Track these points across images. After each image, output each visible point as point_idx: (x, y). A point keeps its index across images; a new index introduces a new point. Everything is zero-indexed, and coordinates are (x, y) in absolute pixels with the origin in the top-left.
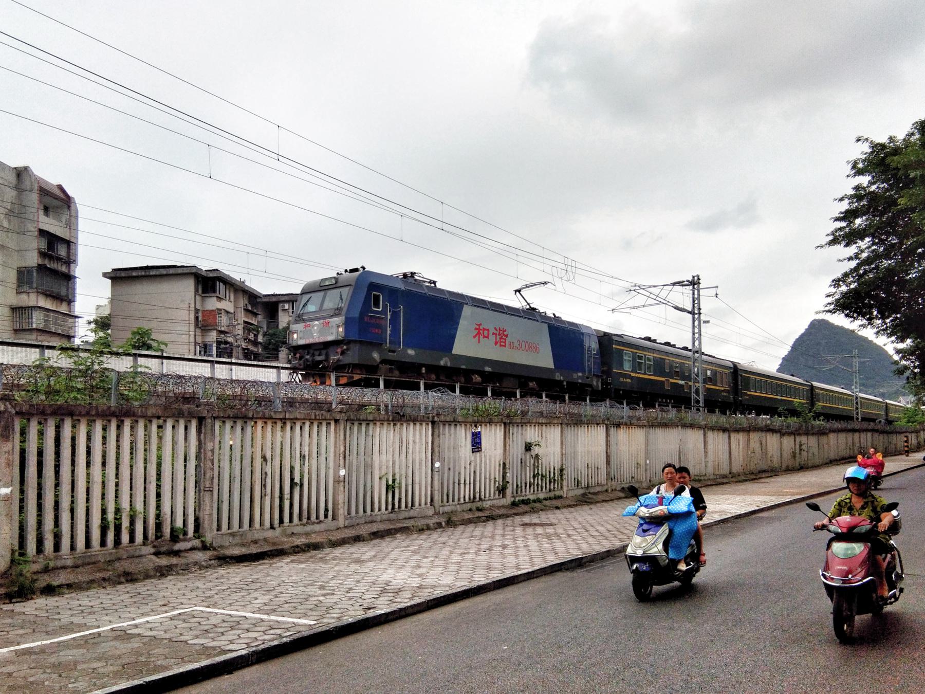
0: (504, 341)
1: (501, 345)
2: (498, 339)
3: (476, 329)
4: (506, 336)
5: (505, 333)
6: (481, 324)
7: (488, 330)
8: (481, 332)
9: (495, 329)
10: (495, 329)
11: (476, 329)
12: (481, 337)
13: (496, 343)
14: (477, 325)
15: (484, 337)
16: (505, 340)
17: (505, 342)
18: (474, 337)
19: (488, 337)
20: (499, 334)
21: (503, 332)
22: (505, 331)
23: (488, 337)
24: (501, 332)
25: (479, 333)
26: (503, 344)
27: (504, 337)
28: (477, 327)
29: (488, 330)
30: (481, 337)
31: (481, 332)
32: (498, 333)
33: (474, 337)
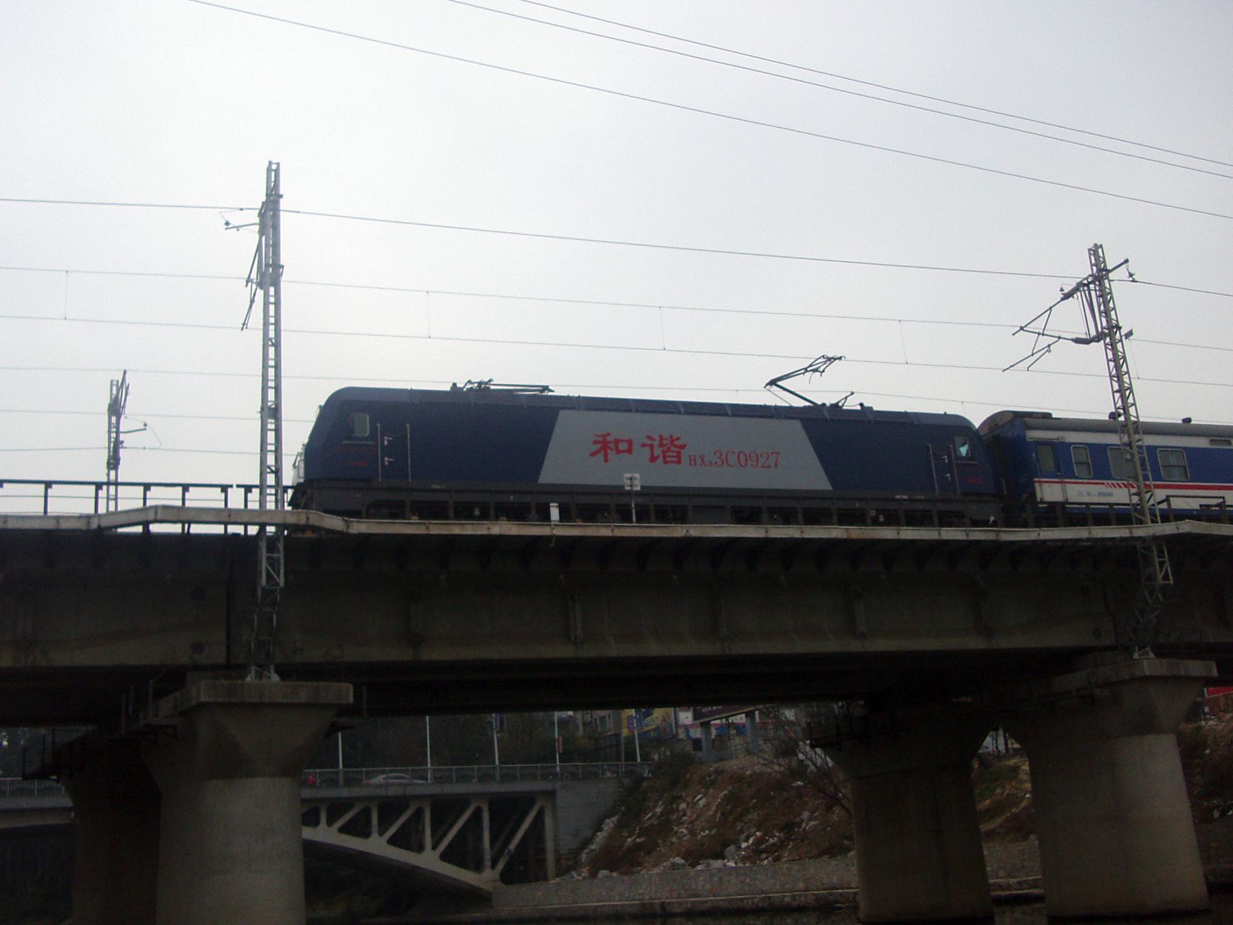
0: (675, 454)
3: (595, 442)
6: (609, 434)
9: (649, 437)
13: (653, 459)
16: (679, 453)
22: (678, 439)
26: (676, 459)
27: (673, 449)
28: (600, 439)
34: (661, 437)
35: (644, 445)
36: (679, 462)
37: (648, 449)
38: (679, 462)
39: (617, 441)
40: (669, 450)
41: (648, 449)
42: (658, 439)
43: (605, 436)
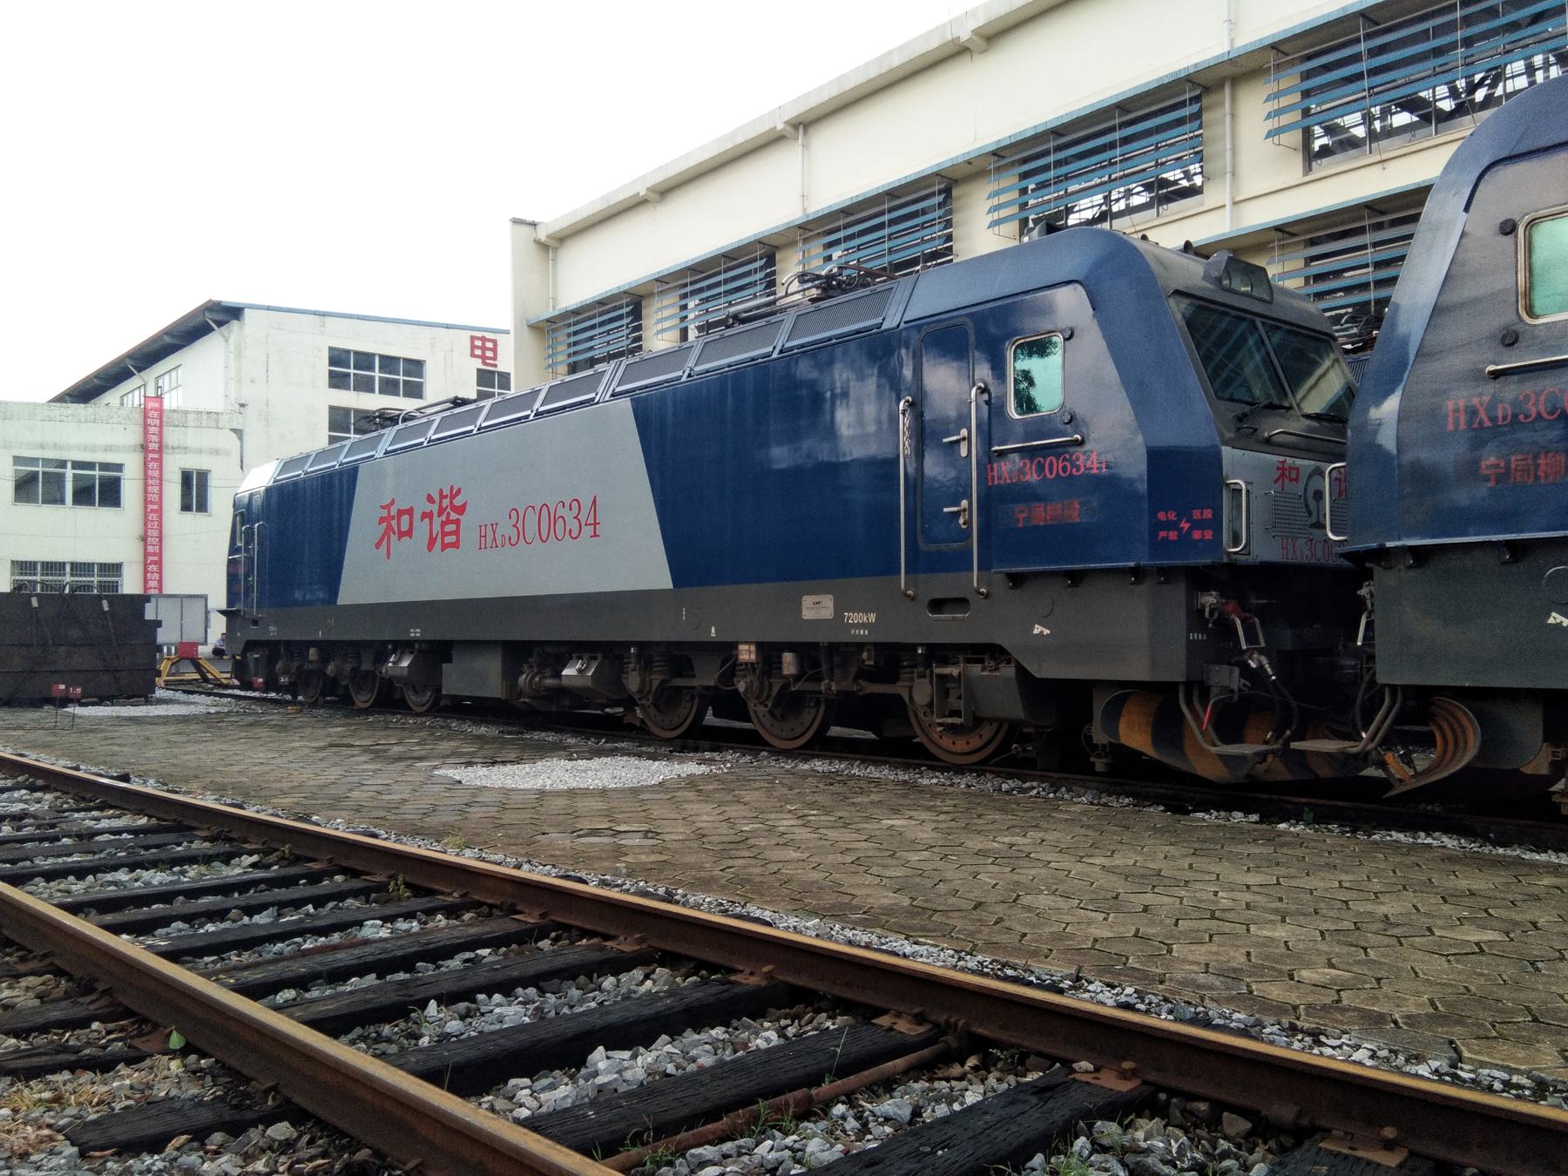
1: (444, 546)
2: (437, 528)
4: (461, 510)
5: (458, 502)
6: (393, 502)
7: (410, 512)
8: (394, 523)
9: (430, 499)
10: (430, 499)
11: (381, 520)
12: (394, 538)
14: (383, 507)
15: (401, 535)
16: (457, 522)
17: (456, 533)
18: (378, 545)
19: (409, 533)
20: (440, 514)
21: (453, 497)
22: (459, 491)
23: (409, 533)
24: (446, 502)
25: (389, 529)
26: (449, 539)
27: (454, 516)
28: (384, 513)
29: (410, 512)
30: (394, 538)
31: (394, 523)
32: (435, 508)
33: (378, 545)
34: (441, 491)
35: (424, 515)
36: (456, 545)
37: (427, 520)
38: (456, 545)
39: (401, 513)
40: (448, 521)
41: (427, 520)
42: (437, 498)
43: (387, 507)
